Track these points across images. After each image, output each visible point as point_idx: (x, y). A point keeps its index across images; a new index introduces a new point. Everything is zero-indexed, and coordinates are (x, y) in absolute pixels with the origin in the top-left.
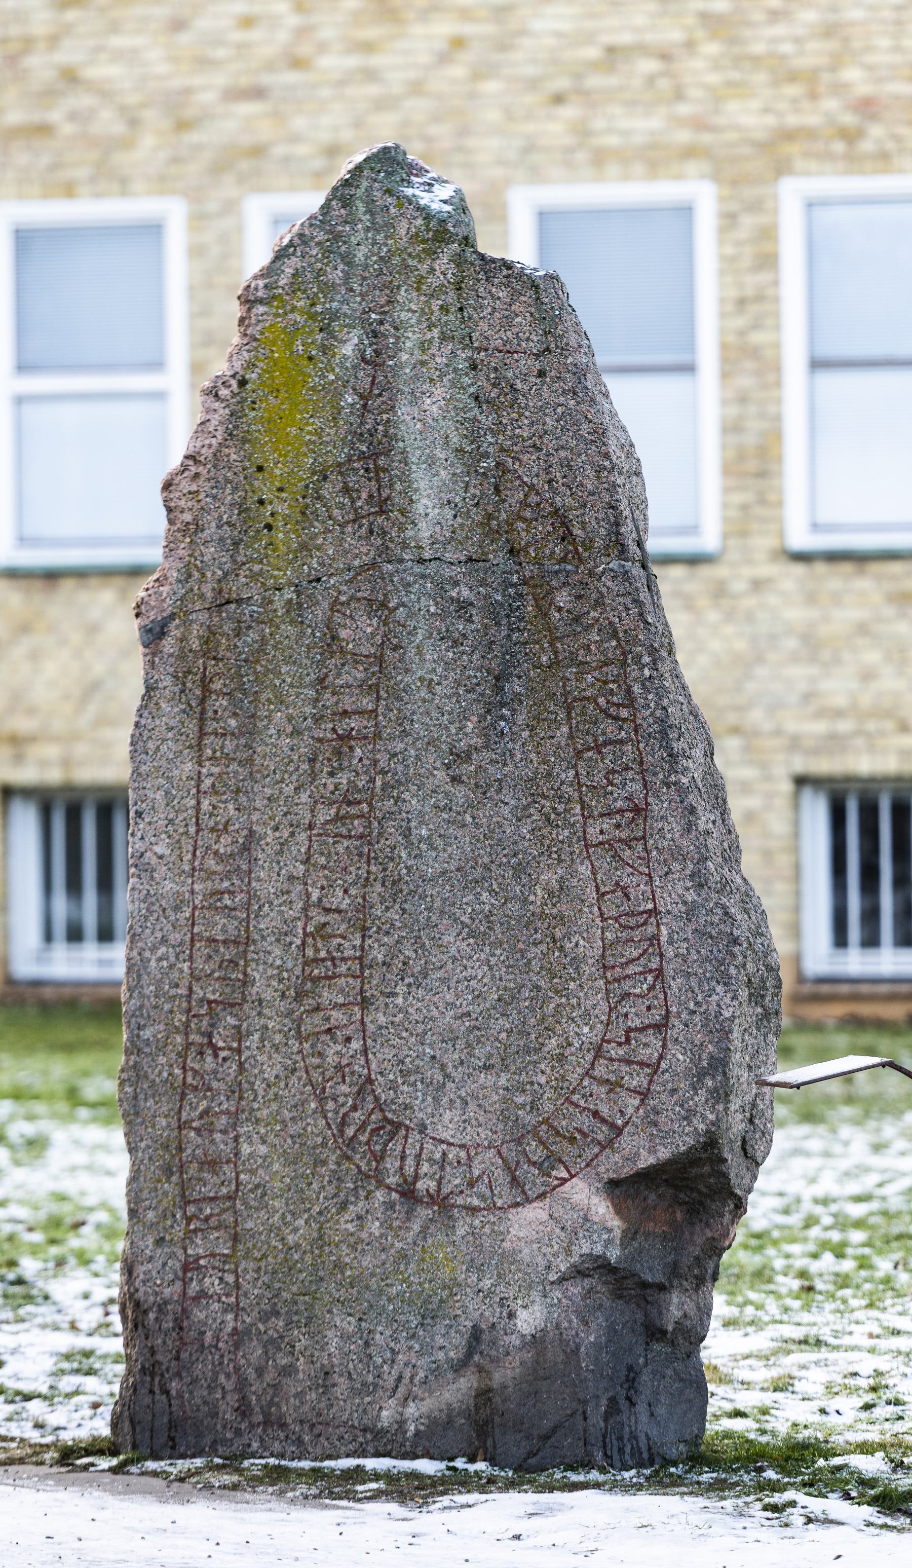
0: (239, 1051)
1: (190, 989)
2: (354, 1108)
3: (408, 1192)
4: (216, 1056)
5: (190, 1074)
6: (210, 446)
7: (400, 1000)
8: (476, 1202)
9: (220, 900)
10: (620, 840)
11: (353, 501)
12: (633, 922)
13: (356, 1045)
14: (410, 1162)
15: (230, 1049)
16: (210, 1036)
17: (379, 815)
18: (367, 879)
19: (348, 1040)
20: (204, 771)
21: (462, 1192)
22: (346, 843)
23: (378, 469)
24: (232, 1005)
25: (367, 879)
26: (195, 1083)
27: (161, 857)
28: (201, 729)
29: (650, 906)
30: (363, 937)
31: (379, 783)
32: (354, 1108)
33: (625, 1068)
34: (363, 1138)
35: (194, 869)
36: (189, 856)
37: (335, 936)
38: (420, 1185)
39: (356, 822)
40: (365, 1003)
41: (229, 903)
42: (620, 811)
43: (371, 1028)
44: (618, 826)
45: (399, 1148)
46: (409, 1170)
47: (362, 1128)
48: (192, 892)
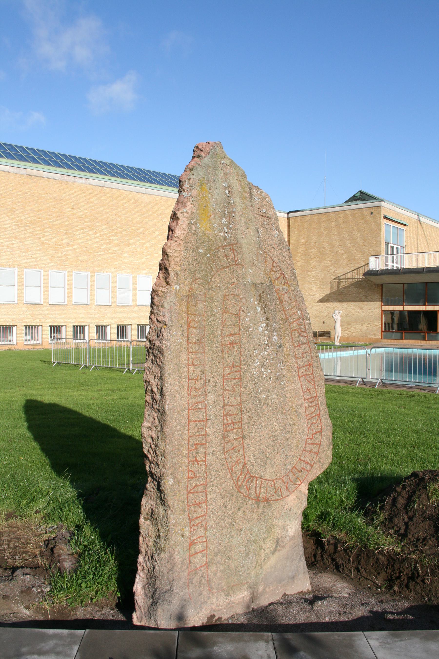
0: (205, 461)
1: (189, 441)
2: (241, 474)
3: (257, 500)
4: (198, 464)
5: (190, 473)
6: (183, 234)
7: (253, 435)
8: (277, 498)
9: (197, 406)
10: (307, 375)
11: (227, 259)
12: (311, 400)
13: (241, 452)
14: (258, 488)
15: (202, 461)
16: (196, 457)
17: (243, 370)
18: (241, 394)
19: (239, 451)
20: (190, 357)
21: (273, 495)
22: (234, 381)
23: (233, 249)
24: (203, 444)
25: (241, 394)
26: (192, 476)
27: (177, 391)
28: (188, 341)
29: (315, 395)
30: (242, 414)
31: (242, 359)
32: (241, 474)
33: (312, 446)
34: (244, 484)
35: (188, 395)
36: (187, 390)
37: (233, 415)
38: (261, 496)
39: (237, 373)
40: (243, 437)
41: (200, 407)
42: (306, 365)
43: (246, 445)
44: (306, 370)
45: (254, 486)
46: (258, 491)
47: (244, 481)
48: (188, 403)
